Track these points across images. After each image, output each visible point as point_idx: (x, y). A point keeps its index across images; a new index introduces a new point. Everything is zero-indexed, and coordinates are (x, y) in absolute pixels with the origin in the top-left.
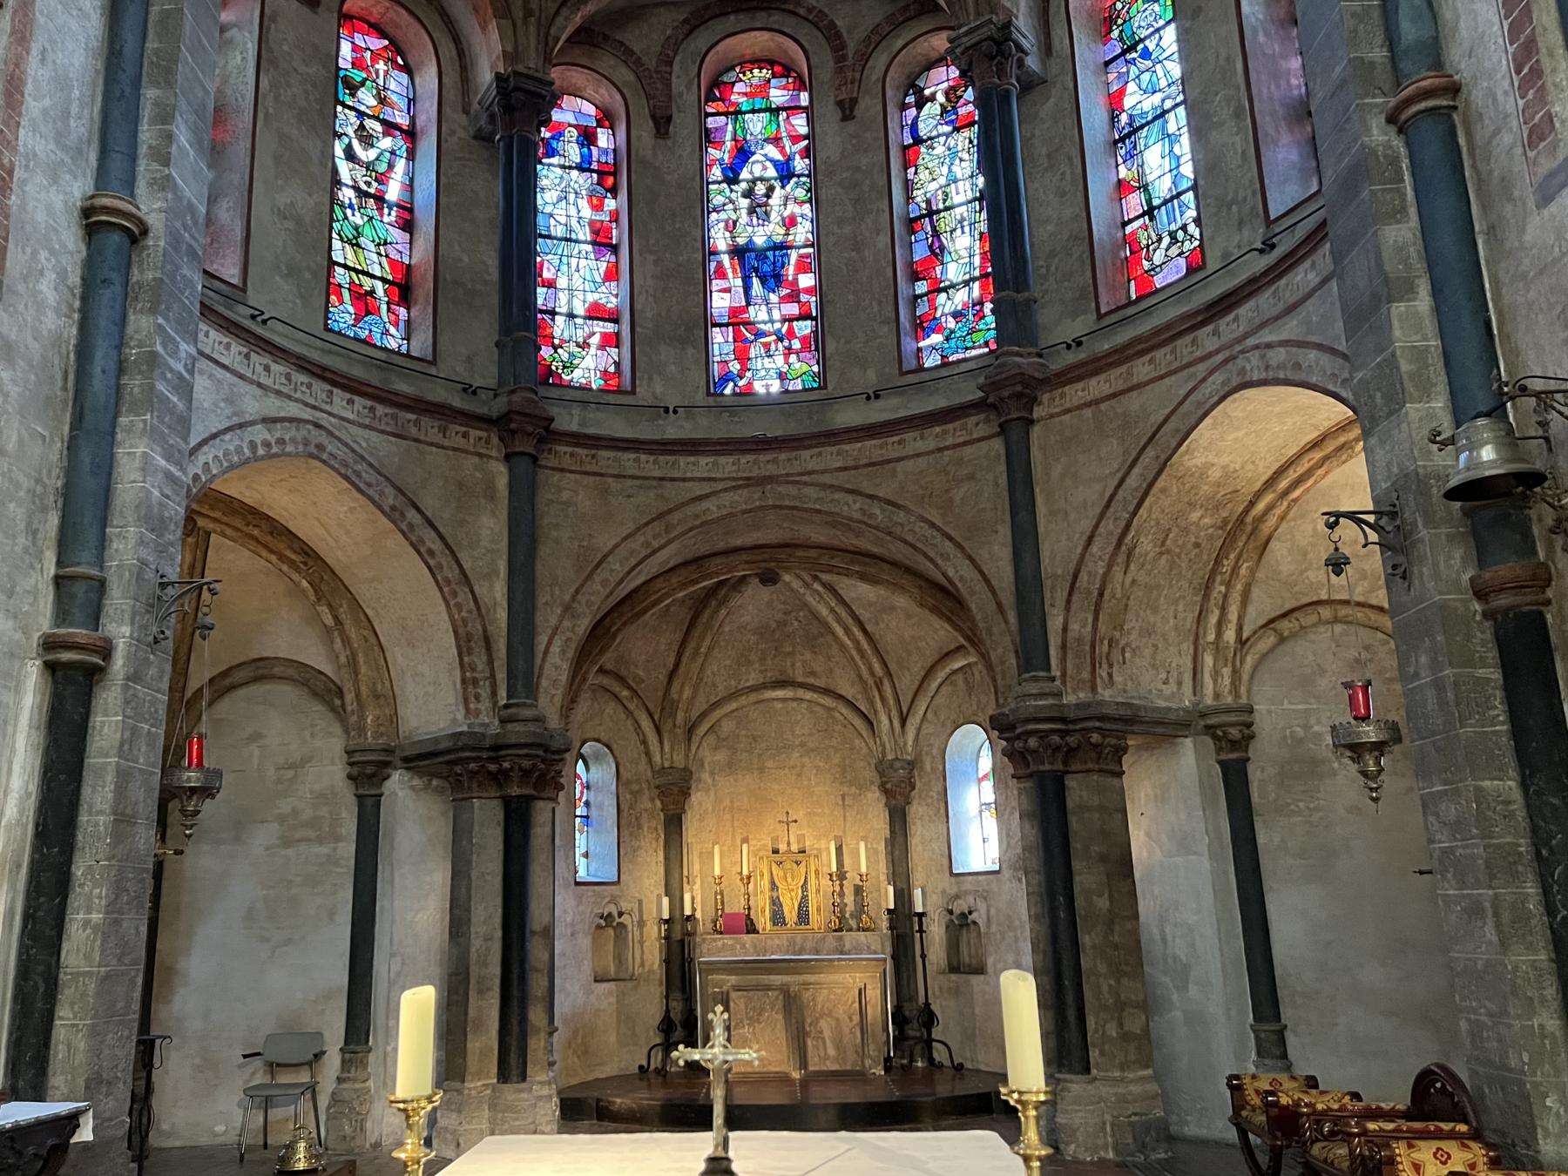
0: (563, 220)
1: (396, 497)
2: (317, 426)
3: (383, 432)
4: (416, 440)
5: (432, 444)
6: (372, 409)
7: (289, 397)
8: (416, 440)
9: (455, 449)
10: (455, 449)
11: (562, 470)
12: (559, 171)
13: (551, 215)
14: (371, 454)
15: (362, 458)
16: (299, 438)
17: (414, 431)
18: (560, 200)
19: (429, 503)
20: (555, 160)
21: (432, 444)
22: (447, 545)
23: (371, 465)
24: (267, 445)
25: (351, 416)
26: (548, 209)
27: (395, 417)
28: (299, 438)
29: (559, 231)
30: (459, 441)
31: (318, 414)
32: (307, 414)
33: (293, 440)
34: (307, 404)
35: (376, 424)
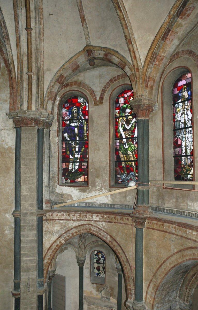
0: (183, 121)
1: (110, 239)
2: (89, 224)
3: (106, 222)
4: (115, 223)
5: (119, 223)
6: (103, 217)
7: (81, 220)
8: (115, 223)
9: (125, 224)
10: (125, 224)
11: (154, 229)
12: (181, 104)
13: (180, 121)
14: (104, 228)
15: (101, 230)
16: (84, 229)
17: (114, 220)
18: (182, 114)
19: (118, 239)
20: (180, 101)
21: (119, 223)
22: (123, 251)
23: (103, 231)
24: (76, 232)
25: (98, 220)
26: (179, 119)
27: (109, 217)
28: (84, 229)
29: (182, 126)
30: (126, 221)
31: (88, 222)
32: (86, 222)
33: (83, 230)
34: (86, 220)
35: (104, 220)
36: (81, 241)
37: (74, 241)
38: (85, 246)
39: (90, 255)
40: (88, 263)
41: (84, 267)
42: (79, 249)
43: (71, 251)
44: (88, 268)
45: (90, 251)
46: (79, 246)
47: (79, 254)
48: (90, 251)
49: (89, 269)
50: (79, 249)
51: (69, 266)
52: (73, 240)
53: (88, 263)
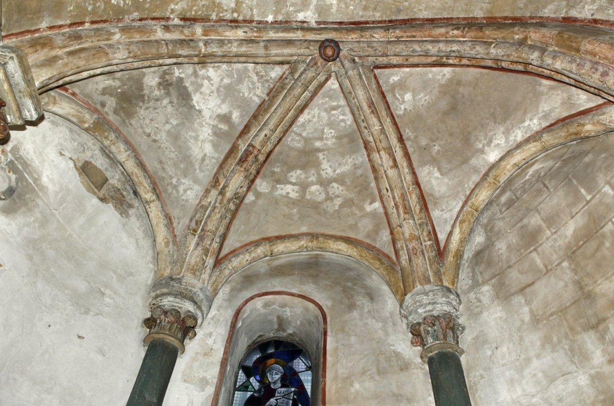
36: (214, 193)
37: (181, 189)
38: (222, 254)
39: (229, 314)
40: (208, 353)
41: (181, 364)
42: (190, 237)
43: (137, 240)
44: (204, 382)
45: (240, 290)
46: (193, 224)
47: (179, 261)
48: (235, 291)
49: (210, 390)
50: (190, 237)
51: (87, 312)
52: (174, 181)
53: (208, 353)
